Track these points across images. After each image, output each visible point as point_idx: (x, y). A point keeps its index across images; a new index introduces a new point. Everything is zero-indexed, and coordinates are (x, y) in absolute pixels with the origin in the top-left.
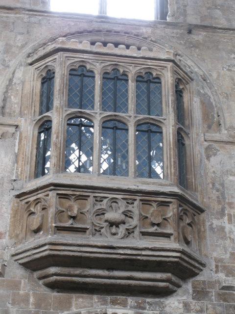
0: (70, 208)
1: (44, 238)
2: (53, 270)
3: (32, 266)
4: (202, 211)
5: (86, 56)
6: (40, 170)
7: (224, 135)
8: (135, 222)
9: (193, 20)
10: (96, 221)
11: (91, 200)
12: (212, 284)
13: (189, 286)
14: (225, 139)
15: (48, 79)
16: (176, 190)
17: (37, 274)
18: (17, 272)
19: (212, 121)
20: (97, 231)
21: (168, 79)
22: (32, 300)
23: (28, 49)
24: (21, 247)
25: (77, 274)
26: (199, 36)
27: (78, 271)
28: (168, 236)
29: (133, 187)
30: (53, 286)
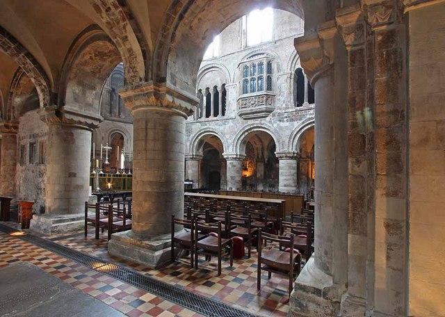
3: (240, 115)
19: (279, 70)
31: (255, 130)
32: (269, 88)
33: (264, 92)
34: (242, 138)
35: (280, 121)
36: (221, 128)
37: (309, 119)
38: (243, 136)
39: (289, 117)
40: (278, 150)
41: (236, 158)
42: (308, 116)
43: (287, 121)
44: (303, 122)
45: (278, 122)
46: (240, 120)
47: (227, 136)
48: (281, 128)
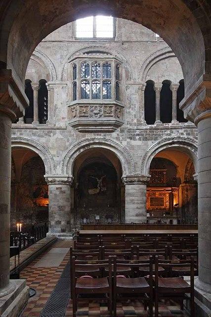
0: (83, 110)
1: (77, 119)
2: (80, 127)
3: (74, 126)
4: (124, 107)
5: (86, 59)
6: (75, 99)
8: (102, 113)
10: (91, 113)
11: (89, 107)
12: (126, 128)
13: (119, 129)
14: (132, 83)
15: (75, 68)
16: (115, 102)
17: (75, 129)
18: (70, 128)
19: (128, 77)
20: (91, 116)
21: (113, 65)
22: (75, 135)
27: (87, 128)
28: (112, 116)
29: (102, 103)
30: (80, 131)
31: (95, 146)
32: (117, 98)
33: (112, 101)
34: (75, 156)
35: (131, 138)
36: (43, 140)
37: (166, 140)
38: (78, 153)
39: (142, 135)
40: (124, 176)
41: (67, 181)
43: (140, 139)
44: (158, 144)
45: (128, 140)
46: (74, 132)
47: (53, 152)
48: (132, 147)
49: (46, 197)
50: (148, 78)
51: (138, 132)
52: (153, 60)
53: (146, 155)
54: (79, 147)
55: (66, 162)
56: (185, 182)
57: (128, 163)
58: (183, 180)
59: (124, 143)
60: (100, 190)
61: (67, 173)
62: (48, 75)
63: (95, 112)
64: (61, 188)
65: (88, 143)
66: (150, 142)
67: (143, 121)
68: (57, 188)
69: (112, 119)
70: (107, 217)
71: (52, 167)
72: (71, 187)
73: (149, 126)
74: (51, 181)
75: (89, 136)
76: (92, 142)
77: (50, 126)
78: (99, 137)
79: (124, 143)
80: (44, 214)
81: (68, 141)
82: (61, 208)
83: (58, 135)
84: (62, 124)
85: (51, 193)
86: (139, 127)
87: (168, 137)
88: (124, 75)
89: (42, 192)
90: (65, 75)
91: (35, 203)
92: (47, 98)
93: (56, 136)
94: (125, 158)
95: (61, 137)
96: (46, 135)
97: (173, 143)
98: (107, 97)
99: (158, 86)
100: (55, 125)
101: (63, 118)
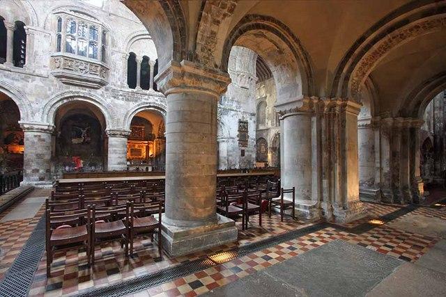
1: (59, 70)
3: (58, 77)
7: (117, 49)
9: (112, 12)
13: (104, 87)
15: (60, 21)
19: (114, 45)
21: (100, 30)
23: (52, 8)
24: (53, 71)
25: (70, 81)
26: (112, 17)
33: (98, 61)
36: (18, 84)
37: (144, 103)
38: (60, 103)
41: (47, 130)
42: (143, 101)
43: (123, 99)
44: (138, 105)
45: (112, 98)
46: (56, 81)
48: (116, 105)
49: (21, 143)
50: (131, 51)
51: (121, 93)
52: (139, 35)
53: (128, 113)
54: (63, 97)
55: (47, 110)
56: (159, 138)
57: (112, 118)
58: (157, 136)
59: (109, 101)
60: (84, 140)
61: (48, 121)
62: (27, 19)
63: (82, 68)
64: (40, 136)
65: (72, 95)
66: (131, 103)
67: (126, 84)
68: (35, 136)
69: (98, 78)
70: (91, 165)
71: (29, 114)
72: (52, 135)
73: (131, 90)
74: (28, 129)
75: (73, 89)
76: (76, 95)
77: (28, 71)
78: (84, 92)
79: (109, 101)
80: (18, 162)
81: (50, 89)
82: (39, 156)
83: (38, 81)
84: (43, 72)
85: (28, 139)
86: (122, 89)
87: (146, 101)
88: (110, 42)
89: (17, 138)
90: (48, 25)
91: (7, 150)
92: (25, 41)
93: (35, 83)
94: (108, 113)
95: (41, 84)
96: (23, 79)
97: (150, 106)
98: (93, 57)
99: (139, 59)
100: (34, 71)
101: (44, 66)
